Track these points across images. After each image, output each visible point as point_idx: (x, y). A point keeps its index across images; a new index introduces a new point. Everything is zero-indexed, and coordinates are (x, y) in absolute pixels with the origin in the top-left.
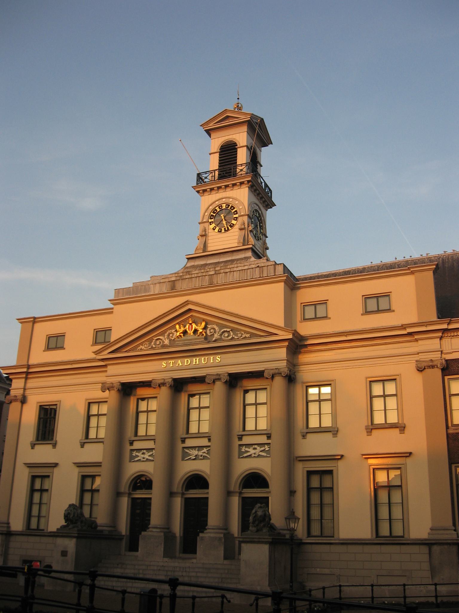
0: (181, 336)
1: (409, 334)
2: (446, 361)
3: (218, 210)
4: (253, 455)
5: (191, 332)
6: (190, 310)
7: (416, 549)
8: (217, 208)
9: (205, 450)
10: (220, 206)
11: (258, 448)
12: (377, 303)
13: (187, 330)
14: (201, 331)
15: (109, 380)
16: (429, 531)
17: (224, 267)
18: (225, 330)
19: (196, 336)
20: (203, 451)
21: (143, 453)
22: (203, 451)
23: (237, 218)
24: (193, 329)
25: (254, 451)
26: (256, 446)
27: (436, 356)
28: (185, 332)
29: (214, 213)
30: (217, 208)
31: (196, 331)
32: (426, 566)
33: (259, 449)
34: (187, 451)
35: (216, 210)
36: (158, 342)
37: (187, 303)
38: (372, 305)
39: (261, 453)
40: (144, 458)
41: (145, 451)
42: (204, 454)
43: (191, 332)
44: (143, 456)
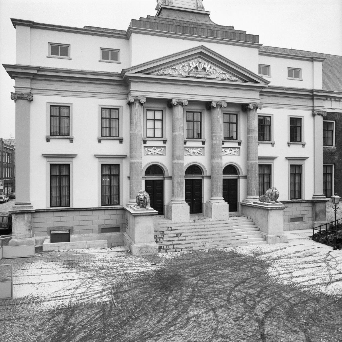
1: (312, 95)
4: (229, 154)
5: (200, 69)
6: (201, 53)
7: (307, 205)
9: (199, 149)
11: (233, 150)
13: (198, 67)
16: (312, 196)
17: (184, 22)
19: (205, 73)
20: (198, 150)
21: (155, 149)
22: (198, 150)
24: (202, 67)
25: (231, 152)
26: (231, 149)
28: (196, 68)
31: (204, 69)
32: (310, 212)
33: (233, 150)
34: (187, 149)
36: (173, 71)
37: (202, 47)
39: (234, 153)
40: (155, 153)
41: (155, 148)
42: (199, 152)
43: (200, 69)
44: (155, 151)
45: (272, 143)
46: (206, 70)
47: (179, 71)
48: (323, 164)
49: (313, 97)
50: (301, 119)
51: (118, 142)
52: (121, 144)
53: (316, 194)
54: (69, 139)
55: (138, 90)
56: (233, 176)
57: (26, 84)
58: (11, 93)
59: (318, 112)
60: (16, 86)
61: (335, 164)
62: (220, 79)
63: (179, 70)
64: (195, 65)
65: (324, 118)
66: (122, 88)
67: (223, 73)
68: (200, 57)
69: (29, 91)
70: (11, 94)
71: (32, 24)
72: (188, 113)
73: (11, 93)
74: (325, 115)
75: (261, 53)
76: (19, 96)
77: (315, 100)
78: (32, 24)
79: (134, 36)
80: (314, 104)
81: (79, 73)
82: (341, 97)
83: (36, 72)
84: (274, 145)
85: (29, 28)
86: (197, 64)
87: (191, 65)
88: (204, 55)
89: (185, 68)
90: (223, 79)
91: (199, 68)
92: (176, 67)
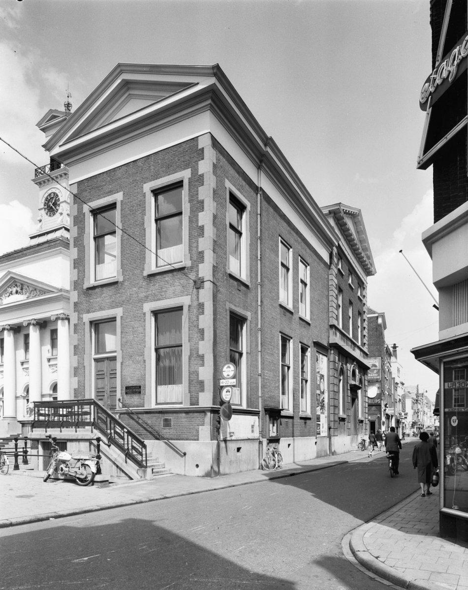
10: (50, 195)
23: (59, 204)
29: (46, 201)
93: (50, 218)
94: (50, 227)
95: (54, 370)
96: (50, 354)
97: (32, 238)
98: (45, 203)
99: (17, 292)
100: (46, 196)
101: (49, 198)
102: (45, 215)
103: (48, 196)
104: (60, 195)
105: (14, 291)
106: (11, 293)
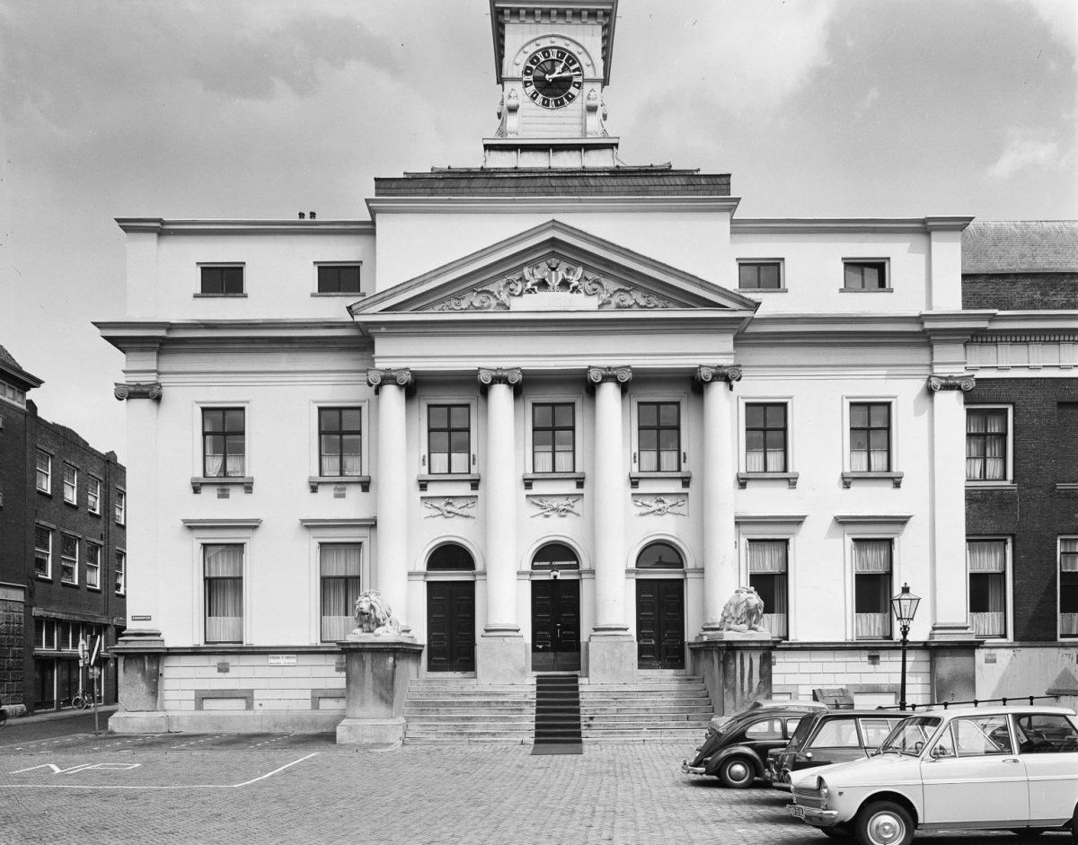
0: (533, 290)
1: (922, 335)
2: (977, 380)
3: (542, 59)
8: (540, 55)
10: (545, 51)
12: (872, 272)
13: (547, 279)
14: (576, 283)
15: (380, 364)
18: (622, 287)
23: (580, 83)
27: (958, 371)
30: (540, 55)
35: (538, 60)
36: (482, 297)
38: (856, 277)
45: (788, 479)
46: (571, 286)
47: (498, 296)
48: (966, 535)
49: (929, 337)
50: (784, 405)
51: (359, 488)
52: (365, 494)
53: (941, 621)
54: (242, 484)
55: (394, 354)
56: (660, 573)
57: (147, 361)
58: (116, 384)
59: (946, 378)
60: (128, 369)
61: (1013, 536)
62: (613, 305)
63: (499, 292)
64: (539, 276)
65: (969, 398)
66: (355, 356)
67: (620, 290)
68: (553, 254)
69: (152, 378)
70: (115, 387)
71: (158, 225)
72: (642, 407)
73: (116, 384)
74: (971, 385)
75: (741, 228)
76: (132, 389)
77: (935, 346)
78: (158, 225)
79: (382, 222)
80: (932, 358)
81: (272, 326)
82: (1075, 330)
83: (162, 333)
84: (795, 484)
85: (155, 235)
86: (546, 274)
87: (527, 276)
88: (557, 250)
89: (512, 286)
90: (620, 307)
91: (549, 283)
92: (491, 288)
93: (546, 112)
94: (553, 135)
95: (651, 509)
96: (635, 467)
97: (488, 147)
98: (528, 68)
99: (565, 284)
100: (532, 49)
101: (542, 59)
102: (528, 99)
103: (537, 52)
104: (583, 59)
105: (554, 281)
106: (543, 284)
